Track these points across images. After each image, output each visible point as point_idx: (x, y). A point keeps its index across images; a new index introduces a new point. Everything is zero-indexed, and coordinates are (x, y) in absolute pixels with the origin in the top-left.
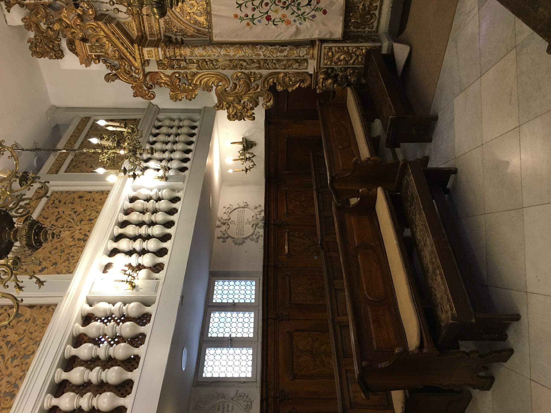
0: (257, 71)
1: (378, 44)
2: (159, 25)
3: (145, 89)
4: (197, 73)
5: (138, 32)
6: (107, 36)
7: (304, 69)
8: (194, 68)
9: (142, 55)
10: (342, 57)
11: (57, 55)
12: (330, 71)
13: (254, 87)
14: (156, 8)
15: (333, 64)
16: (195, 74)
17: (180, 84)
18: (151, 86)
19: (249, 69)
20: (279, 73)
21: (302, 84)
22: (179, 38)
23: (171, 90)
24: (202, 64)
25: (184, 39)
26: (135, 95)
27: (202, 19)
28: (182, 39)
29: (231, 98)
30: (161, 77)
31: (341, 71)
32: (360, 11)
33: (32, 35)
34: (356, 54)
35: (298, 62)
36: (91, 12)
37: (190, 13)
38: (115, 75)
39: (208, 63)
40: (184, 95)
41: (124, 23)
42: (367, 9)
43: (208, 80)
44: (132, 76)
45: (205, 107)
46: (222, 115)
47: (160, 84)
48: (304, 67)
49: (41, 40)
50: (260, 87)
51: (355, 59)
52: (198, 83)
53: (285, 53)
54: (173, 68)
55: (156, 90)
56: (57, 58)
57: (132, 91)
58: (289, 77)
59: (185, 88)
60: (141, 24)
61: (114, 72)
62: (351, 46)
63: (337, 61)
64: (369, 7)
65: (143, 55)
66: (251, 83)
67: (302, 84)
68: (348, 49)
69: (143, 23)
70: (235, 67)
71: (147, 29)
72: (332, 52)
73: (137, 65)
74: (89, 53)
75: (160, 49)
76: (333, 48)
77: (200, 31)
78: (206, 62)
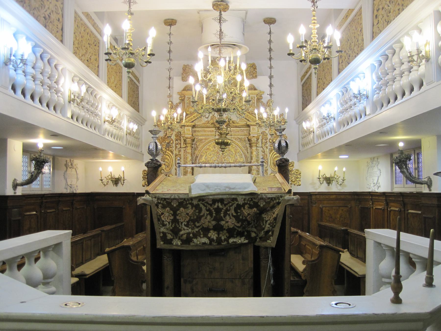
4: (173, 154)
9: (188, 126)
16: (172, 152)
22: (193, 146)
27: (203, 159)
45: (143, 155)
54: (177, 140)
59: (164, 145)
61: (174, 107)
75: (191, 136)
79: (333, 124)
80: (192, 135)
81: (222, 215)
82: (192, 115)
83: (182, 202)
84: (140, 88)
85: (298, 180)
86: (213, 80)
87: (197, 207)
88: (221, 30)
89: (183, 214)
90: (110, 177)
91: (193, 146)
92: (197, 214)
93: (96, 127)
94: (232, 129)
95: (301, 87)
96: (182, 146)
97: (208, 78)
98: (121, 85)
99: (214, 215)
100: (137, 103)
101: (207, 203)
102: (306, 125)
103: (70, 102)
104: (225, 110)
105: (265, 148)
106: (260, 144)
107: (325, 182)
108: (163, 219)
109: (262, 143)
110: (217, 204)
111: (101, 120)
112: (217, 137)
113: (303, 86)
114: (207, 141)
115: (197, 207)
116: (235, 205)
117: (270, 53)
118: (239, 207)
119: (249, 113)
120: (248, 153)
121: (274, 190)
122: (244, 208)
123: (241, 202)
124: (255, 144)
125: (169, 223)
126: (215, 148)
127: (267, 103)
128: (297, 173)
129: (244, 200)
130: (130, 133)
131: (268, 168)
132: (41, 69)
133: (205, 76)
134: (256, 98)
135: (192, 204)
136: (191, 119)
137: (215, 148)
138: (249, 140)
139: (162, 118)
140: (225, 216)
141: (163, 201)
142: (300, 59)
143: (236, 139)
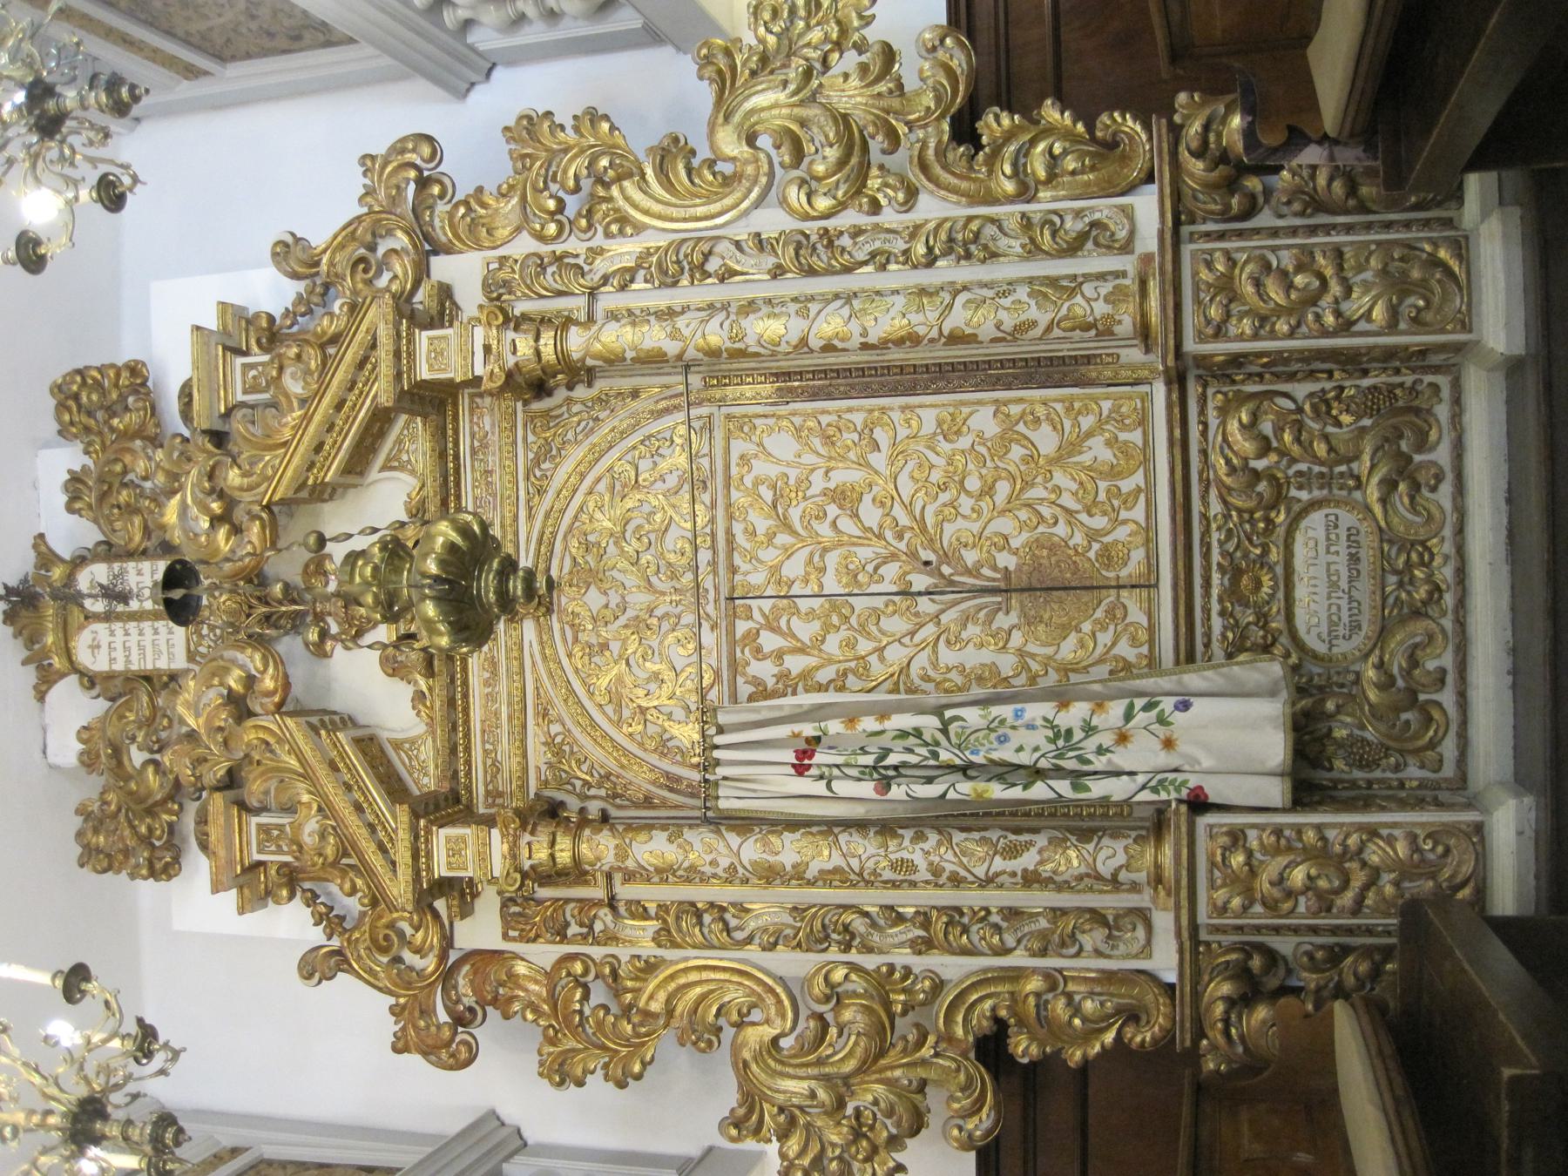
0: (919, 963)
1: (1470, 816)
2: (525, 755)
3: (443, 1016)
5: (440, 780)
6: (307, 776)
7: (1136, 957)
8: (640, 938)
10: (1298, 876)
11: (158, 866)
12: (1256, 963)
13: (904, 1038)
14: (431, 598)
15: (1258, 908)
16: (650, 967)
17: (587, 1011)
18: (471, 1010)
19: (881, 952)
20: (1016, 975)
21: (1129, 1032)
22: (594, 808)
23: (545, 1036)
24: (679, 922)
25: (613, 812)
26: (400, 1046)
28: (603, 811)
30: (512, 976)
31: (1315, 967)
32: (1373, 695)
33: (90, 788)
34: (1364, 864)
35: (1106, 924)
36: (269, 684)
37: (643, 710)
38: (339, 952)
39: (707, 918)
40: (597, 1063)
41: (397, 745)
42: (1400, 683)
43: (703, 997)
44: (398, 960)
47: (503, 1005)
48: (1136, 948)
49: (119, 810)
50: (931, 1039)
51: (1366, 888)
52: (655, 1007)
53: (1028, 860)
54: (561, 935)
55: (488, 1033)
56: (153, 874)
57: (390, 1026)
58: (1069, 996)
60: (454, 749)
61: (336, 943)
62: (1336, 823)
63: (1276, 893)
64: (1407, 674)
65: (429, 855)
66: (892, 1017)
67: (1129, 1032)
68: (1323, 838)
69: (468, 749)
70: (818, 940)
72: (1250, 854)
73: (395, 892)
74: (257, 857)
75: (495, 832)
76: (1252, 834)
77: (679, 779)
78: (699, 915)
80: (489, 822)
84: (270, 1152)
91: (594, 808)
96: (599, 893)
105: (602, 266)
106: (576, 305)
119: (320, 393)
120: (635, 394)
127: (295, 276)
128: (775, 13)
131: (741, 232)
143: (541, 492)
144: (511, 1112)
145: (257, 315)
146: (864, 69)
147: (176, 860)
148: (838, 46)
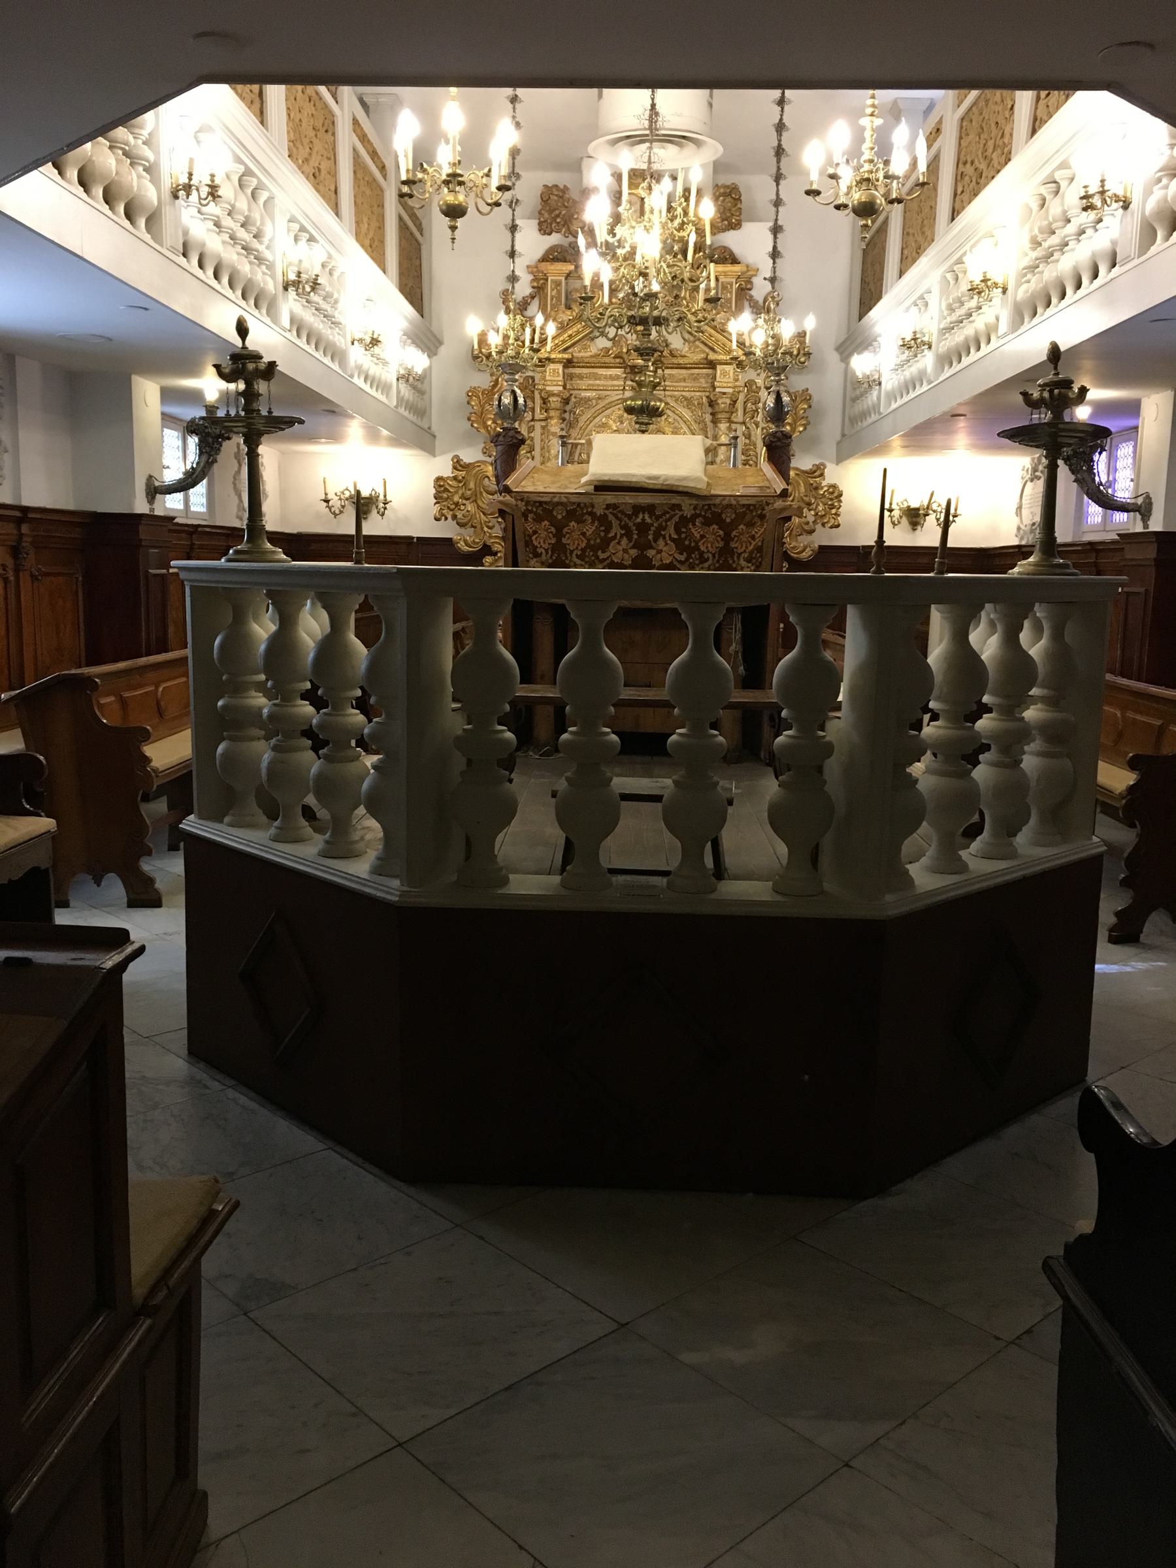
22: (566, 416)
29: (472, 485)
45: (435, 436)
46: (447, 471)
56: (540, 224)
71: (577, 371)
75: (561, 388)
79: (927, 360)
80: (564, 387)
81: (650, 537)
82: (565, 331)
83: (574, 511)
84: (423, 248)
85: (834, 511)
86: (630, 241)
87: (603, 520)
88: (653, 106)
89: (576, 534)
90: (347, 494)
91: (566, 416)
92: (602, 534)
93: (337, 354)
94: (667, 371)
95: (860, 254)
96: (538, 416)
97: (618, 237)
98: (382, 242)
99: (635, 537)
100: (418, 291)
101: (622, 512)
102: (861, 364)
103: (286, 289)
104: (658, 321)
106: (739, 416)
107: (905, 520)
108: (536, 543)
109: (745, 413)
110: (641, 516)
111: (344, 337)
112: (628, 394)
113: (865, 252)
114: (602, 404)
115: (603, 520)
116: (676, 519)
117: (778, 161)
118: (684, 521)
119: (714, 328)
121: (752, 491)
122: (694, 525)
123: (688, 512)
124: (727, 415)
125: (547, 551)
126: (622, 423)
127: (765, 301)
128: (832, 493)
129: (695, 508)
130: (406, 377)
132: (229, 204)
133: (612, 232)
134: (735, 286)
135: (592, 514)
136: (564, 342)
137: (622, 423)
138: (712, 403)
139: (495, 340)
140: (655, 541)
141: (537, 508)
142: (836, 203)
143: (676, 401)
144: (443, 350)
145: (751, 283)
146: (808, 523)
147: (545, 233)
148: (816, 514)
